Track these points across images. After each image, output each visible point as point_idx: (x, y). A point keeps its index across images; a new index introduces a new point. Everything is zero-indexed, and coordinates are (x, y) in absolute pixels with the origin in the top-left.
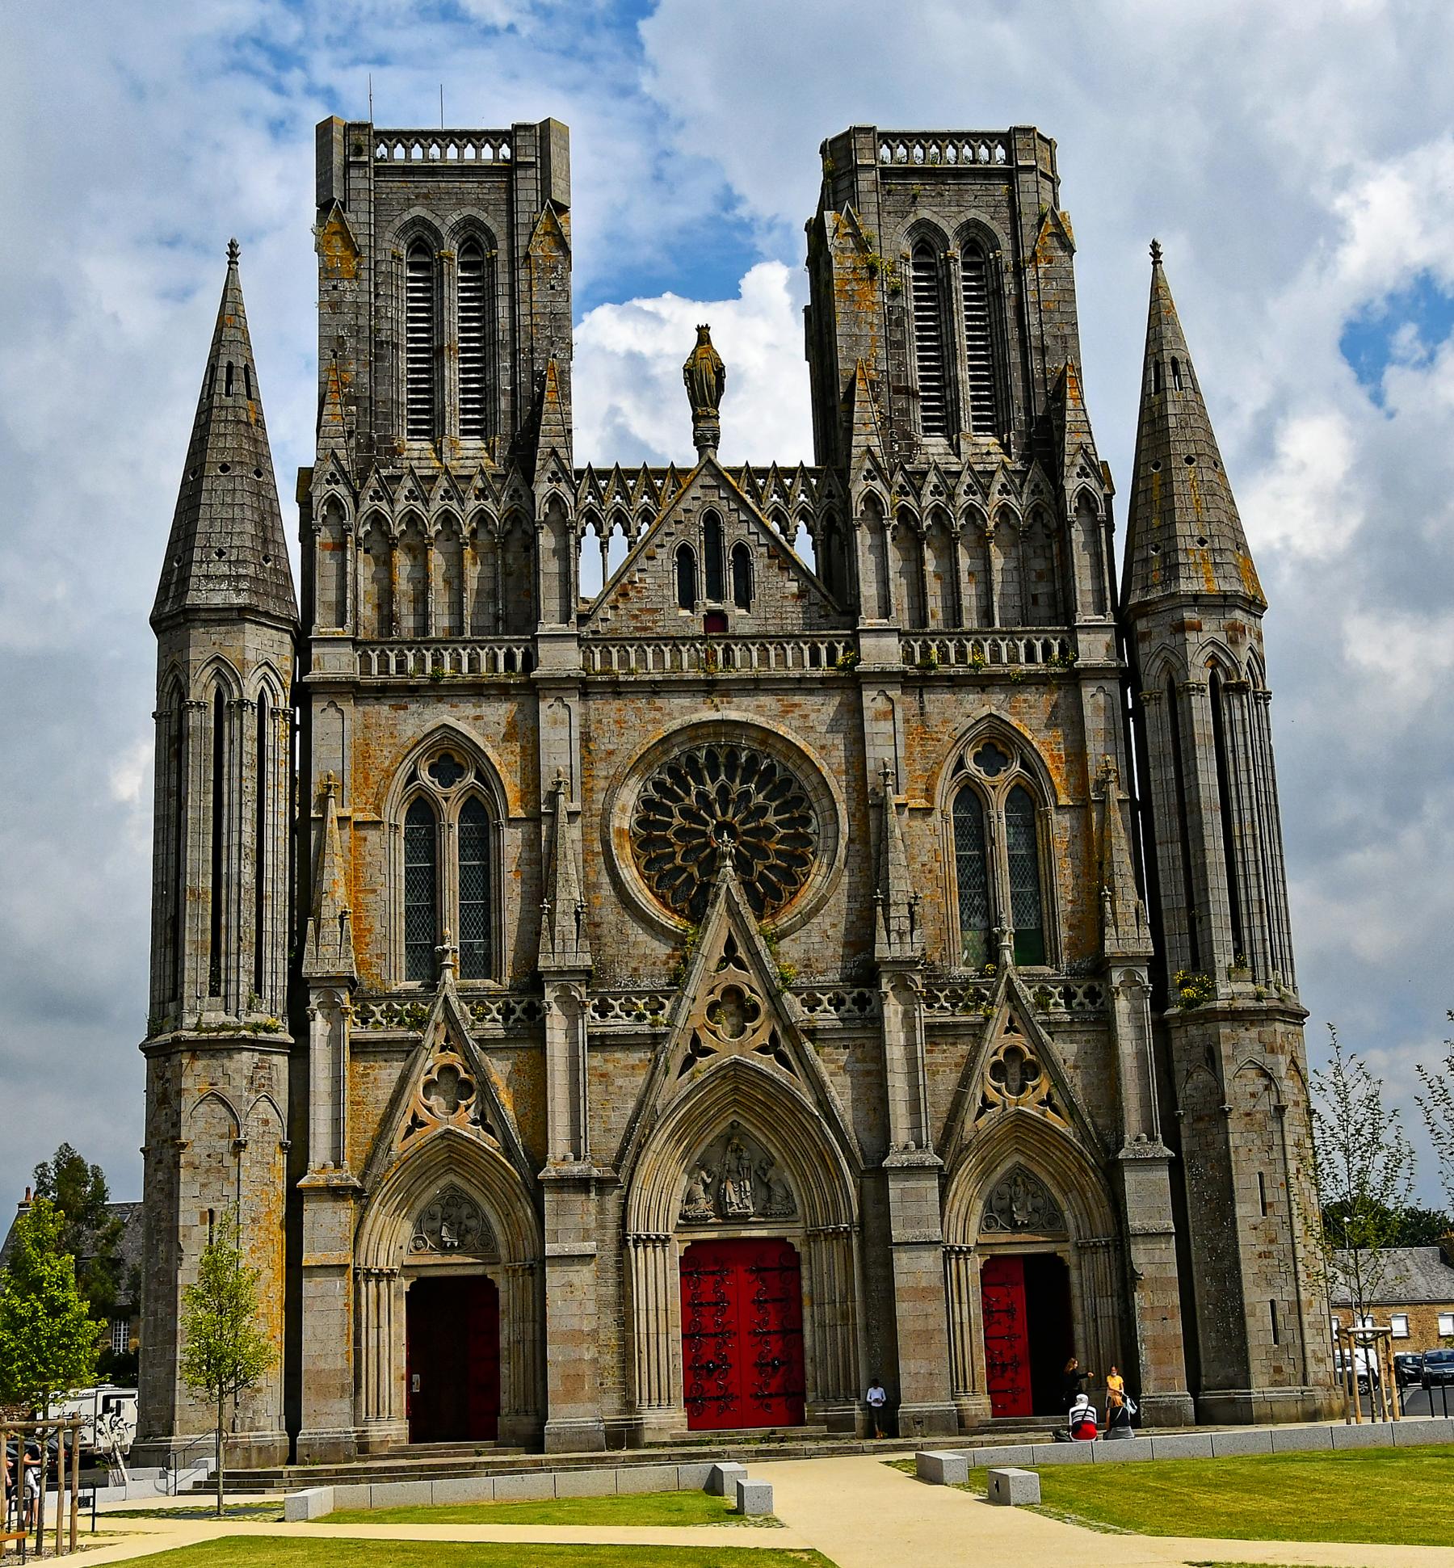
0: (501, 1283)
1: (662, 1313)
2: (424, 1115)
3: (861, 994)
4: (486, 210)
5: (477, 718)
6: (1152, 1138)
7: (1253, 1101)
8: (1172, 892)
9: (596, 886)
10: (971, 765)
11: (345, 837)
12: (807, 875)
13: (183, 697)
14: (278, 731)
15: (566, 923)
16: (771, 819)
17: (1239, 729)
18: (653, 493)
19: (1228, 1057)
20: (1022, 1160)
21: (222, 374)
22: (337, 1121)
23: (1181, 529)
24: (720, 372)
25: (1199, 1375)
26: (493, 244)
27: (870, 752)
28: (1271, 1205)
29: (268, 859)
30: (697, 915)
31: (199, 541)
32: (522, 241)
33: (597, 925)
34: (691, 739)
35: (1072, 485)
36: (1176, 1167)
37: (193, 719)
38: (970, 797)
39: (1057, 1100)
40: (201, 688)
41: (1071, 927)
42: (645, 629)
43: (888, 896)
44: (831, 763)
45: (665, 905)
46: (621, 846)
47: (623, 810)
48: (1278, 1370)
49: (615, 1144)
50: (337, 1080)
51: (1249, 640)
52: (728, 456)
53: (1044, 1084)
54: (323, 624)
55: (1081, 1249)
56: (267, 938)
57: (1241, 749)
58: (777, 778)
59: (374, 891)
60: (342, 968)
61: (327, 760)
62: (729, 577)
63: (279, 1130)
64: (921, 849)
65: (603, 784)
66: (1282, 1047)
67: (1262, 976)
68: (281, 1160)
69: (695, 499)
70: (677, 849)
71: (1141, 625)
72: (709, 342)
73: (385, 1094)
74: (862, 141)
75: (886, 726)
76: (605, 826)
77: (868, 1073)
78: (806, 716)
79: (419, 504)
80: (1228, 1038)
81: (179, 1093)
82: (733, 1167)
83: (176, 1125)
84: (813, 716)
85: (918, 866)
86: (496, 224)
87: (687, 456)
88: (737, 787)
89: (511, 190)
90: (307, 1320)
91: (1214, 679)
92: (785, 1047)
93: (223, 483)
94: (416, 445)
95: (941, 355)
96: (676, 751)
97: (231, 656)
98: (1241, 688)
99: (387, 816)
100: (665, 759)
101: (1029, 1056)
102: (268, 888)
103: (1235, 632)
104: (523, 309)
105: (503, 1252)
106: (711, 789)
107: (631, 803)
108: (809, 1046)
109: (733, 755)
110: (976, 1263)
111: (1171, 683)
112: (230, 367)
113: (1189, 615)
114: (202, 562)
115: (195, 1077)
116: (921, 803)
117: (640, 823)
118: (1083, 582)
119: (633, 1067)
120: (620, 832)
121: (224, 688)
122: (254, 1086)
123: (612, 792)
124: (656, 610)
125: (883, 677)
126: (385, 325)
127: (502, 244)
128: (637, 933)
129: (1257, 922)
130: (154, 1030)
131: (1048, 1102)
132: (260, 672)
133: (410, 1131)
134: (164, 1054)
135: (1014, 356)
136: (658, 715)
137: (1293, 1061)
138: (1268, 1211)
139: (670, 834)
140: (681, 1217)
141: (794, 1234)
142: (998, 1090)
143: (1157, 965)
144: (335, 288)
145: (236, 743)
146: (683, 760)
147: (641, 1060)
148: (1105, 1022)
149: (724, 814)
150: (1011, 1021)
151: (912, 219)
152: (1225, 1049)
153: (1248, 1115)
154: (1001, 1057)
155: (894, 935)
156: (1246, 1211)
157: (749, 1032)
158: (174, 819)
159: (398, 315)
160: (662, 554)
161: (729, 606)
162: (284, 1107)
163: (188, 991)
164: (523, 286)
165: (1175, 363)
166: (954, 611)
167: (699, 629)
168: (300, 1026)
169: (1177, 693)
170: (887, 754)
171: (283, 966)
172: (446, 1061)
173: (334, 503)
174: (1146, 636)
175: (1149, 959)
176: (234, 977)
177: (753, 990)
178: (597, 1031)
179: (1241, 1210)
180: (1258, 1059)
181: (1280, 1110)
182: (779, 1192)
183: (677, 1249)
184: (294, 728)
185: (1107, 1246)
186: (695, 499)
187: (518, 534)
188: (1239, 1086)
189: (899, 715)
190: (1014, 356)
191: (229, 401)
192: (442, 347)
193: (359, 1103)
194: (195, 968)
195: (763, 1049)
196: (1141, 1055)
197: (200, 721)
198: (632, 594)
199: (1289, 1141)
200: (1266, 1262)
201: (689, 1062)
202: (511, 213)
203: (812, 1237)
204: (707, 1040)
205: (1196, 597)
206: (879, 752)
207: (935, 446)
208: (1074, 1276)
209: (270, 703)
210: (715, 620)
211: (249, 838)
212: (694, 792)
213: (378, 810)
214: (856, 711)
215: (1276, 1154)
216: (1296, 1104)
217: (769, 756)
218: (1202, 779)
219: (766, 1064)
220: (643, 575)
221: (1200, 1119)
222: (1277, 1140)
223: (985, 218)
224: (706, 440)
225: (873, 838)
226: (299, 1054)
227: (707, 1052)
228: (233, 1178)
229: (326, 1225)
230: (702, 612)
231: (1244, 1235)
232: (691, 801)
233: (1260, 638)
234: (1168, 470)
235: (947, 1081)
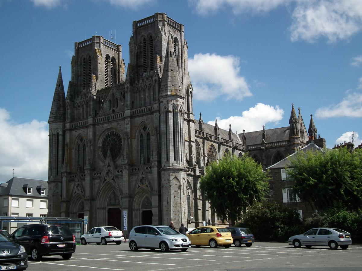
5: (84, 132)
14: (60, 138)
34: (108, 131)
38: (141, 136)
47: (100, 143)
78: (120, 125)
96: (106, 133)
100: (105, 135)
106: (110, 139)
110: (141, 212)
117: (102, 145)
133: (75, 193)
151: (141, 35)
153: (166, 187)
154: (141, 179)
155: (124, 161)
167: (111, 113)
182: (117, 201)
183: (107, 209)
201: (104, 182)
204: (106, 178)
209: (59, 134)
210: (113, 111)
230: (112, 110)
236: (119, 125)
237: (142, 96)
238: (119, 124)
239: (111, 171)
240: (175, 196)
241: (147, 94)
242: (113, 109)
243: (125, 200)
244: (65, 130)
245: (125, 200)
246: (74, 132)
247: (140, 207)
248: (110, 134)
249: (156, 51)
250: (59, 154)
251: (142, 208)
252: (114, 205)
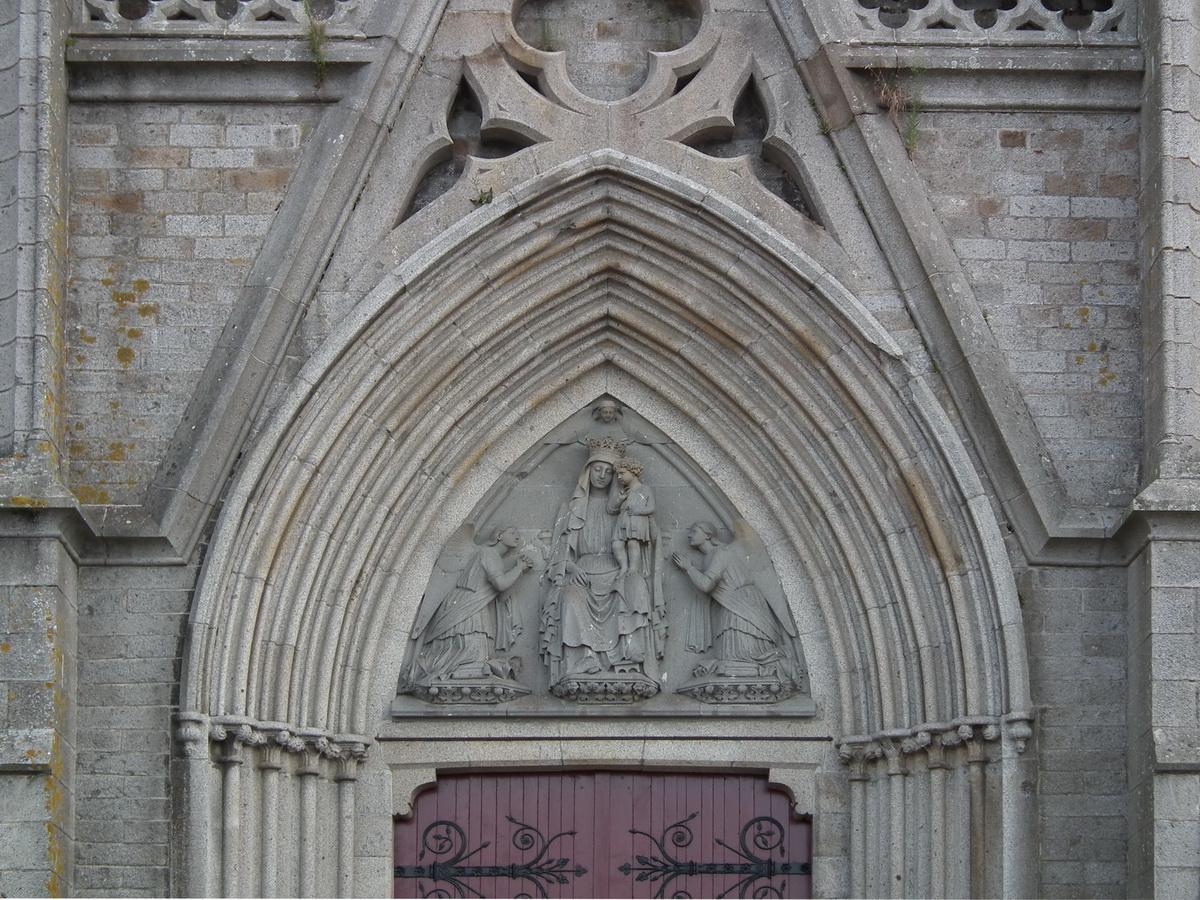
82: (594, 539)
92: (794, 127)
119: (237, 179)
140: (407, 690)
141: (803, 768)
147: (264, 158)
178: (103, 52)
182: (745, 617)
195: (710, 140)
201: (441, 167)
204: (505, 99)
219: (727, 184)
227: (505, 141)
252: (631, 702)
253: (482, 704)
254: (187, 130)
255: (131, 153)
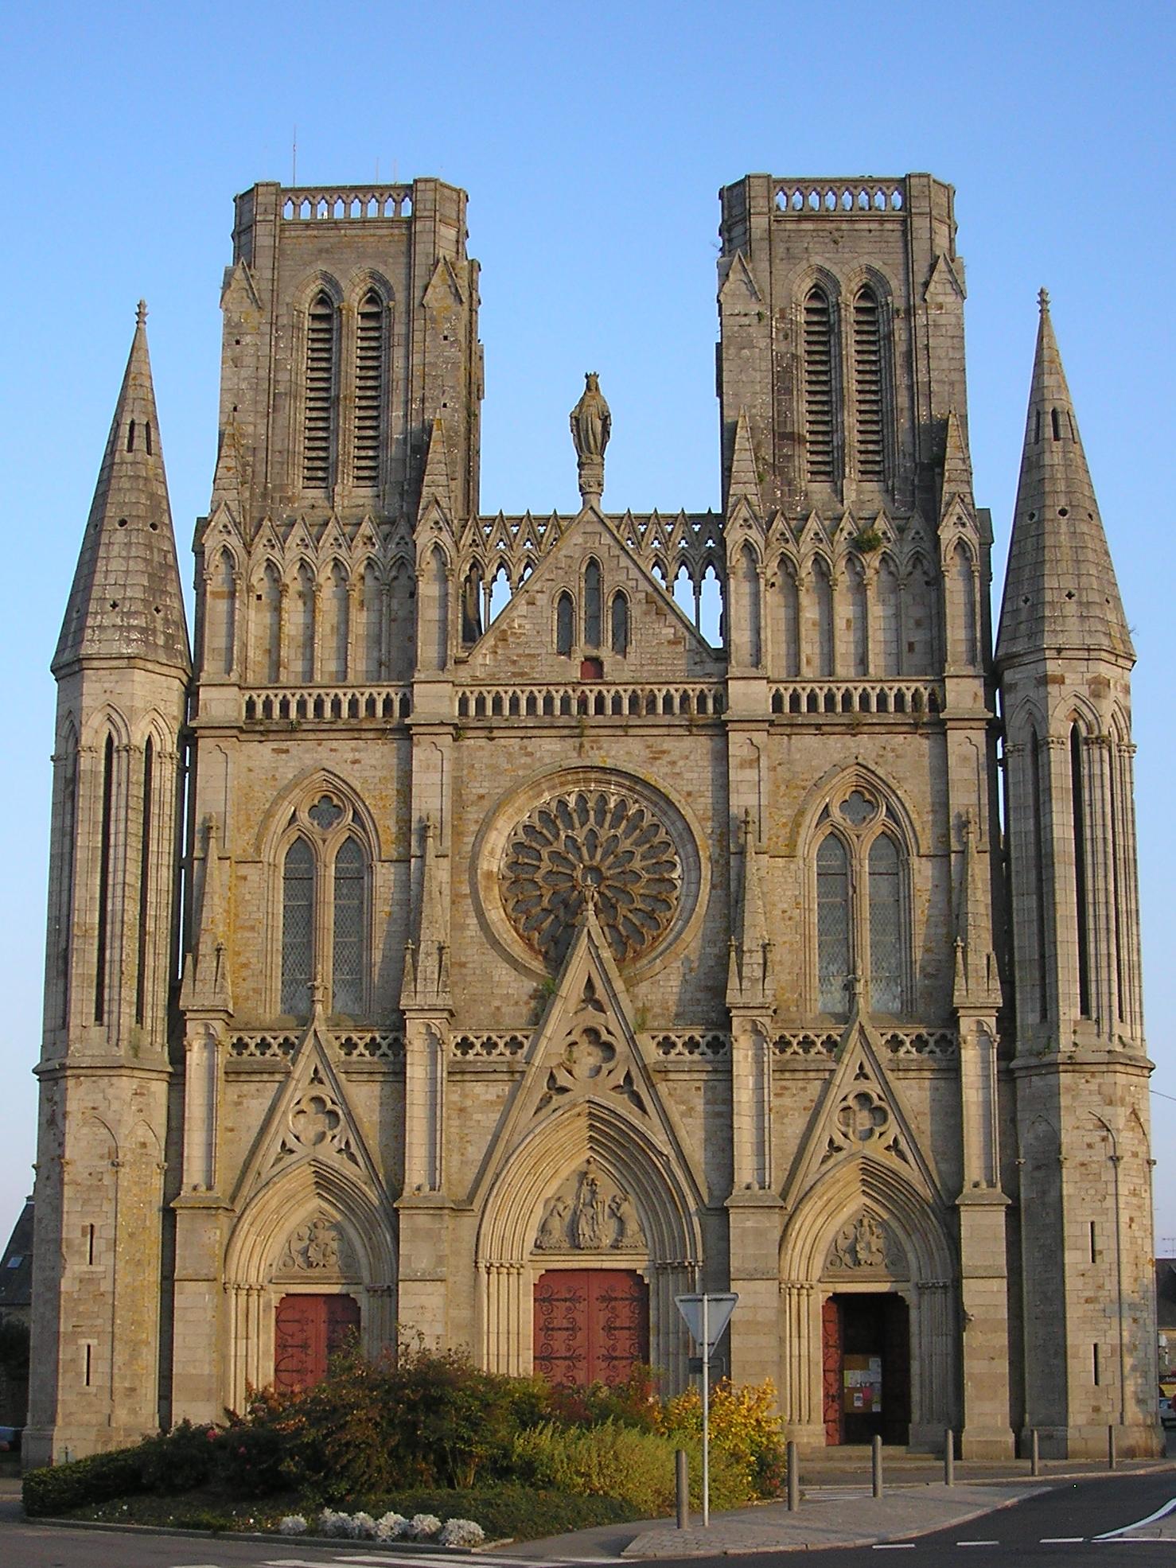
0: (363, 1301)
1: (514, 1337)
2: (292, 1143)
3: (715, 1038)
4: (385, 263)
5: (355, 762)
6: (991, 1184)
7: (1089, 1152)
8: (1024, 941)
9: (463, 927)
10: (836, 813)
11: (225, 877)
12: (669, 921)
13: (77, 741)
14: (165, 774)
15: (428, 964)
16: (637, 864)
17: (1097, 783)
18: (538, 541)
19: (1067, 1108)
20: (868, 1202)
21: (125, 430)
22: (210, 1146)
23: (1050, 582)
24: (606, 420)
25: (1023, 1411)
26: (391, 298)
27: (734, 800)
28: (1101, 1252)
29: (151, 897)
30: (557, 958)
31: (96, 593)
32: (418, 293)
33: (463, 965)
35: (948, 534)
36: (1013, 1213)
37: (85, 763)
39: (903, 1145)
40: (93, 733)
41: (927, 976)
42: (522, 674)
43: (741, 944)
44: (697, 812)
45: (531, 946)
46: (488, 889)
47: (492, 853)
48: (1096, 1409)
49: (471, 1174)
50: (211, 1108)
51: (1114, 693)
52: (611, 504)
53: (893, 1129)
54: (211, 668)
55: (921, 1289)
56: (148, 972)
57: (1099, 805)
58: (645, 824)
59: (252, 928)
60: (217, 1001)
61: (211, 800)
62: (608, 624)
63: (157, 1152)
64: (782, 894)
65: (475, 828)
66: (1122, 1100)
67: (1106, 1029)
68: (158, 1182)
69: (575, 543)
70: (544, 891)
71: (1009, 676)
72: (597, 389)
73: (256, 1124)
74: (758, 189)
75: (751, 774)
76: (473, 868)
77: (718, 1115)
78: (673, 763)
79: (309, 552)
80: (1068, 1089)
81: (65, 1115)
83: (61, 1145)
84: (681, 763)
85: (777, 912)
86: (395, 276)
87: (572, 505)
88: (604, 834)
89: (411, 241)
90: (178, 1328)
91: (1075, 732)
92: (640, 1087)
93: (120, 536)
94: (310, 493)
95: (827, 403)
96: (547, 796)
97: (121, 703)
98: (1101, 741)
99: (267, 856)
101: (877, 1102)
102: (150, 926)
103: (1099, 687)
104: (417, 359)
105: (365, 1274)
106: (580, 836)
107: (501, 845)
108: (662, 1088)
109: (603, 799)
110: (819, 1298)
111: (1034, 734)
112: (132, 424)
113: (1052, 667)
114: (96, 613)
115: (78, 1097)
116: (784, 851)
118: (956, 634)
120: (489, 875)
121: (114, 734)
122: (132, 1109)
123: (480, 836)
124: (533, 656)
125: (749, 722)
126: (283, 376)
127: (400, 296)
128: (503, 972)
129: (1104, 975)
130: (46, 1058)
131: (895, 1147)
132: (148, 718)
134: (52, 1075)
135: (902, 400)
136: (528, 760)
137: (1134, 1112)
138: (1098, 1258)
139: (538, 877)
140: (536, 1246)
142: (845, 1135)
143: (1007, 1017)
144: (238, 342)
145: (124, 786)
146: (554, 804)
148: (952, 1071)
149: (592, 857)
150: (861, 1067)
152: (1065, 1101)
153: (1083, 1165)
155: (745, 983)
156: (1074, 1258)
157: (605, 1072)
158: (67, 857)
159: (297, 364)
160: (542, 600)
161: (606, 653)
162: (162, 1132)
163: (74, 1021)
164: (418, 336)
165: (1054, 413)
166: (829, 658)
167: (576, 674)
168: (178, 1057)
169: (1039, 746)
170: (751, 800)
171: (163, 996)
172: (314, 1093)
173: (226, 552)
174: (1013, 687)
175: (998, 1009)
176: (115, 1009)
177: (609, 1032)
179: (1070, 1257)
180: (1098, 1111)
181: (1115, 1160)
183: (531, 1276)
184: (182, 771)
185: (945, 1287)
186: (575, 543)
187: (403, 580)
188: (1074, 1134)
189: (764, 762)
190: (902, 400)
191: (129, 457)
192: (338, 398)
193: (232, 1130)
194: (82, 1000)
196: (987, 1104)
197: (91, 763)
198: (511, 640)
199: (1123, 1190)
200: (1091, 1306)
201: (546, 1100)
202: (410, 266)
203: (660, 1269)
204: (563, 1079)
205: (1059, 650)
206: (741, 800)
207: (820, 490)
208: (913, 1314)
209: (157, 748)
210: (594, 666)
211: (134, 879)
212: (563, 835)
213: (258, 849)
214: (722, 757)
215: (1110, 1202)
216: (1135, 1155)
217: (636, 801)
218: (1057, 832)
219: (622, 1105)
220: (523, 621)
221: (1038, 1168)
222: (1111, 1189)
223: (877, 265)
224: (589, 489)
225: (733, 885)
226: (177, 1080)
227: (563, 1090)
228: (111, 1195)
229: (199, 1238)
230: (578, 657)
231: (1072, 1283)
232: (560, 846)
233: (1127, 690)
234: (1041, 522)
235: (796, 1126)
236: (666, 758)
237: (810, 611)
238: (664, 752)
239: (605, 1037)
240: (1132, 1220)
241: (844, 610)
242: (594, 653)
243: (749, 1224)
244: (195, 729)
245: (749, 1224)
246: (261, 753)
247: (817, 1272)
248: (572, 801)
249: (922, 377)
250: (152, 885)
251: (827, 1277)
253: (557, 1250)
254: (478, 1088)
255: (464, 1096)
